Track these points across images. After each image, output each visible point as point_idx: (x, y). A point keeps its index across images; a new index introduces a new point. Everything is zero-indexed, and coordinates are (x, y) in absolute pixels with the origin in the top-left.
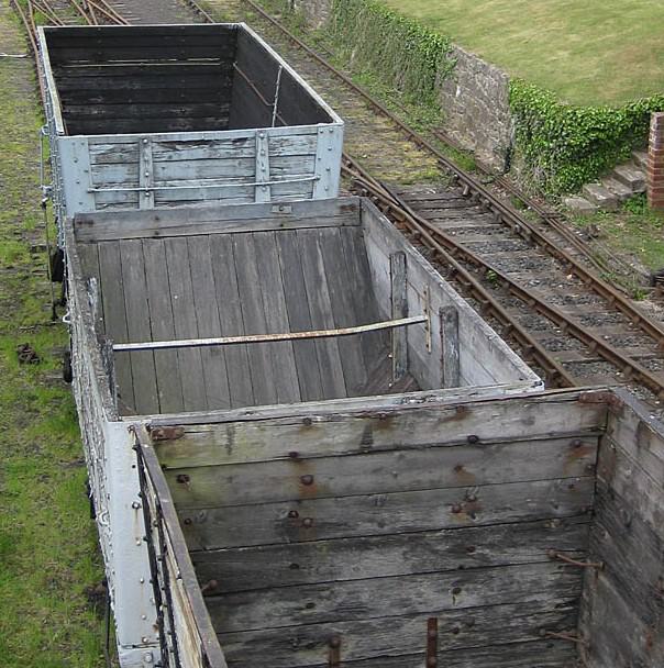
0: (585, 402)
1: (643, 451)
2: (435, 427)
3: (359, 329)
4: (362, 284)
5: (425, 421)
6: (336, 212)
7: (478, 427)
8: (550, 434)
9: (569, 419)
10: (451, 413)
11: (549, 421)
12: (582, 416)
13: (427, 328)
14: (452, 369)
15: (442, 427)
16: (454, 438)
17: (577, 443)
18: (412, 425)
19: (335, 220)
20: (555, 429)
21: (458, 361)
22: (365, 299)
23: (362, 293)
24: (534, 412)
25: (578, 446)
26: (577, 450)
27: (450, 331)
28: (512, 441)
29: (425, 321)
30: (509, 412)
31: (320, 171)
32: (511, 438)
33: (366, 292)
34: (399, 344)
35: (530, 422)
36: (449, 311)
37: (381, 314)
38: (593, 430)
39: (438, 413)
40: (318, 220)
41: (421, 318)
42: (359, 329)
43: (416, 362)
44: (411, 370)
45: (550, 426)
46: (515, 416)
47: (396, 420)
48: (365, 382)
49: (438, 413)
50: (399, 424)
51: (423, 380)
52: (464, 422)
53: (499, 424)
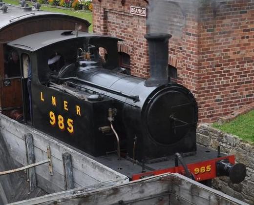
0: (163, 180)
1: (195, 197)
2: (106, 199)
3: (9, 172)
4: (4, 151)
5: (102, 197)
7: (122, 196)
8: (151, 196)
9: (158, 188)
10: (111, 192)
11: (149, 191)
12: (162, 187)
13: (50, 165)
14: (70, 180)
15: (108, 198)
16: (114, 202)
17: (161, 198)
18: (97, 199)
20: (152, 194)
21: (73, 176)
22: (6, 157)
23: (5, 155)
24: (144, 187)
25: (161, 200)
26: (161, 202)
27: (68, 164)
28: (136, 201)
29: (49, 162)
30: (134, 189)
32: (136, 200)
33: (7, 154)
34: (32, 175)
35: (142, 192)
36: (67, 155)
37: (15, 163)
38: (166, 192)
39: (107, 193)
41: (47, 161)
42: (9, 172)
43: (42, 181)
44: (39, 186)
45: (150, 193)
46: (136, 190)
47: (90, 197)
48: (14, 194)
49: (107, 193)
50: (91, 199)
51: (48, 189)
52: (117, 195)
53: (130, 194)
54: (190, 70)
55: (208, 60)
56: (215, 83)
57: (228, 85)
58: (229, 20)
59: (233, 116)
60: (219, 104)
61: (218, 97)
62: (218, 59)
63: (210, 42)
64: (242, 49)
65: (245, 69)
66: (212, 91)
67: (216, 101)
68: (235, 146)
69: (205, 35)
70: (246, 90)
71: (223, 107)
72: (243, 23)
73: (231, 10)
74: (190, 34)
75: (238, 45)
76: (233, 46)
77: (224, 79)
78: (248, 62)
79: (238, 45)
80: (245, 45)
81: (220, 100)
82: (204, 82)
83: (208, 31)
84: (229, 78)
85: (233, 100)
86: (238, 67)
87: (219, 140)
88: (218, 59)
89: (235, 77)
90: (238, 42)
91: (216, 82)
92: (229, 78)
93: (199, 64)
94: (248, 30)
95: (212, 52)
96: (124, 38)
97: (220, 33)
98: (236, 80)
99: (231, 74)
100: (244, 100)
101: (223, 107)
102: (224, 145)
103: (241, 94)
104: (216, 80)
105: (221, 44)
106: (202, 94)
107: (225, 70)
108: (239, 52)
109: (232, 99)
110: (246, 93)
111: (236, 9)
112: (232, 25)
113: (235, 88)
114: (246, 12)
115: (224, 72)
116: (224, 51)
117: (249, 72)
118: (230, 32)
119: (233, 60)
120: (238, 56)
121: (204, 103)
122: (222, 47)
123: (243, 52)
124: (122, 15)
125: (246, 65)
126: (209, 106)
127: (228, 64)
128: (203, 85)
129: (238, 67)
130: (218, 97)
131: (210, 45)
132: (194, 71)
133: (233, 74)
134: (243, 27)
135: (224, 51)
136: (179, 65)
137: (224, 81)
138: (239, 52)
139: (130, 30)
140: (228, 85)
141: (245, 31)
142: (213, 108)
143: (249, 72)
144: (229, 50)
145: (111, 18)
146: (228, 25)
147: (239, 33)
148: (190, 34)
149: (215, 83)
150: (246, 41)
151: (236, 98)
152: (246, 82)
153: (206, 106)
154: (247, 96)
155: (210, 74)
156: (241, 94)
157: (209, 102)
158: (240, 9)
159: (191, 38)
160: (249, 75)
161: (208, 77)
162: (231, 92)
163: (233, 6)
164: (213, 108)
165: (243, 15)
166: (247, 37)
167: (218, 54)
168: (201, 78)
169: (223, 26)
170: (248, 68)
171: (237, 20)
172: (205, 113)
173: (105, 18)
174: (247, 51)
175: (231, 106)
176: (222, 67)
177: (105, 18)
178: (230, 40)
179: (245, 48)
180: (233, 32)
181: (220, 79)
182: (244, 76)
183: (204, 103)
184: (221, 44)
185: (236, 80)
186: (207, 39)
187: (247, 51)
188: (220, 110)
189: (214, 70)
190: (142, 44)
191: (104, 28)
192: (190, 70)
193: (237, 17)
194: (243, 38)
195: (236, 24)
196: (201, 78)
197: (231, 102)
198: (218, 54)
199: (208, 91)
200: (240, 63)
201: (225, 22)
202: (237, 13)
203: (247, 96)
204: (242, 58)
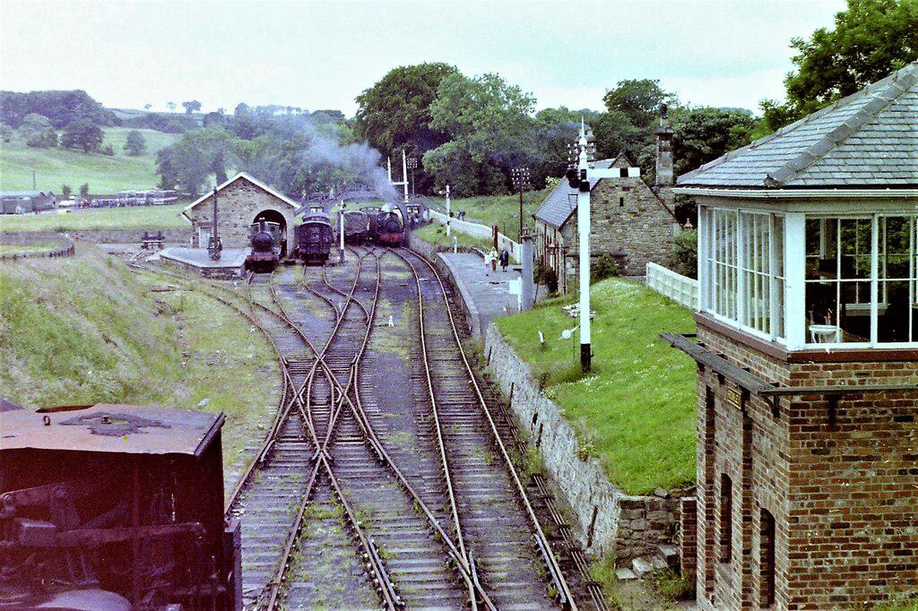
55: (813, 512)
57: (865, 568)
58: (869, 434)
61: (838, 591)
77: (854, 554)
82: (805, 556)
91: (834, 559)
99: (871, 547)
104: (834, 555)
107: (856, 535)
108: (891, 502)
112: (874, 442)
113: (881, 575)
118: (869, 458)
120: (891, 509)
128: (801, 563)
129: (889, 532)
130: (838, 591)
133: (876, 546)
137: (849, 559)
140: (865, 568)
155: (819, 541)
176: (851, 529)
181: (845, 555)
199: (815, 577)
200: (893, 524)
204: (899, 516)
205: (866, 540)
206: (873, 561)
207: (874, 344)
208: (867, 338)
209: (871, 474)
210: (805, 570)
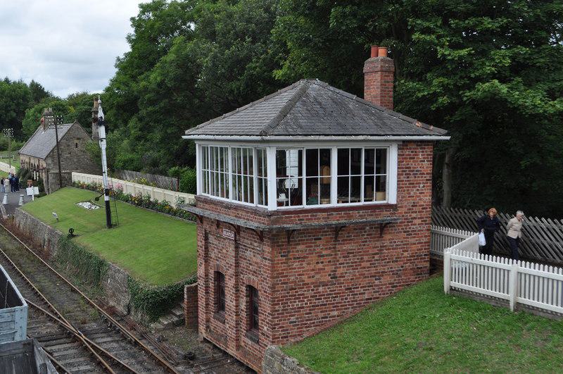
6: (22, 346)
19: (21, 350)
31: (17, 327)
40: (13, 351)
54: (266, 292)
55: (282, 284)
56: (289, 306)
57: (303, 308)
58: (304, 246)
59: (301, 339)
60: (293, 326)
61: (293, 319)
62: (292, 282)
63: (284, 266)
64: (317, 273)
65: (319, 292)
66: (287, 313)
67: (291, 323)
68: (293, 370)
69: (278, 260)
70: (321, 312)
71: (298, 329)
72: (318, 249)
73: (305, 236)
74: (266, 259)
75: (313, 270)
76: (308, 270)
77: (299, 302)
78: (323, 286)
79: (313, 270)
80: (319, 269)
81: (295, 322)
83: (281, 256)
84: (304, 301)
85: (308, 322)
86: (312, 290)
87: (282, 363)
88: (292, 282)
89: (310, 300)
90: (312, 267)
92: (304, 301)
93: (273, 287)
94: (323, 256)
95: (287, 276)
96: (220, 258)
97: (295, 258)
98: (310, 303)
100: (320, 322)
101: (298, 329)
102: (285, 368)
103: (316, 316)
104: (291, 302)
105: (295, 268)
106: (276, 316)
107: (299, 293)
108: (313, 277)
109: (307, 320)
110: (321, 315)
111: (310, 236)
113: (310, 310)
114: (320, 239)
115: (298, 295)
116: (299, 275)
117: (324, 295)
118: (305, 257)
119: (308, 284)
120: (313, 280)
121: (279, 324)
122: (296, 272)
123: (317, 276)
124: (219, 238)
125: (321, 289)
126: (283, 327)
127: (303, 288)
129: (312, 290)
130: (293, 319)
131: (284, 270)
132: (269, 294)
133: (307, 297)
134: (318, 253)
135: (299, 275)
136: (259, 287)
138: (313, 277)
139: (224, 251)
140: (303, 308)
141: (320, 256)
142: (288, 330)
143: (324, 295)
144: (303, 275)
145: (211, 239)
146: (302, 251)
147: (314, 257)
148: (266, 259)
149: (289, 306)
150: (320, 266)
151: (312, 320)
152: (321, 305)
153: (280, 328)
154: (322, 318)
156: (316, 316)
157: (283, 323)
158: (314, 236)
159: (267, 263)
160: (325, 298)
161: (283, 300)
162: (306, 314)
163: (309, 233)
164: (288, 330)
165: (318, 241)
166: (322, 263)
167: (293, 278)
168: (275, 301)
169: (298, 251)
170: (323, 292)
171: (311, 246)
172: (280, 335)
173: (206, 239)
174: (322, 276)
175: (306, 327)
177: (206, 239)
178: (305, 264)
179: (320, 273)
180: (308, 257)
181: (295, 302)
182: (319, 299)
183: (279, 324)
184: (295, 268)
185: (310, 303)
186: (282, 263)
187: (322, 276)
188: (295, 331)
189: (288, 293)
190: (232, 265)
191: (205, 248)
192: (266, 292)
193: (311, 243)
194: (318, 263)
195: (311, 250)
196: (275, 301)
197: (306, 324)
198: (293, 278)
199: (283, 313)
201: (299, 247)
202: (311, 240)
203: (322, 318)
205: (303, 294)
206: (306, 304)
207: (305, 206)
208: (301, 204)
209: (305, 264)
210: (279, 310)
